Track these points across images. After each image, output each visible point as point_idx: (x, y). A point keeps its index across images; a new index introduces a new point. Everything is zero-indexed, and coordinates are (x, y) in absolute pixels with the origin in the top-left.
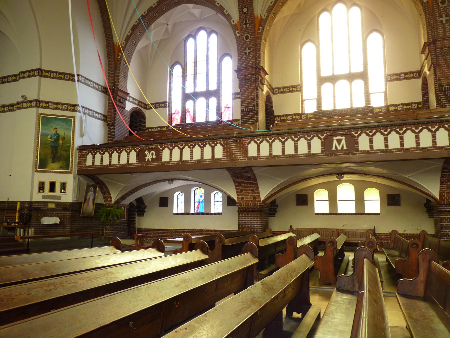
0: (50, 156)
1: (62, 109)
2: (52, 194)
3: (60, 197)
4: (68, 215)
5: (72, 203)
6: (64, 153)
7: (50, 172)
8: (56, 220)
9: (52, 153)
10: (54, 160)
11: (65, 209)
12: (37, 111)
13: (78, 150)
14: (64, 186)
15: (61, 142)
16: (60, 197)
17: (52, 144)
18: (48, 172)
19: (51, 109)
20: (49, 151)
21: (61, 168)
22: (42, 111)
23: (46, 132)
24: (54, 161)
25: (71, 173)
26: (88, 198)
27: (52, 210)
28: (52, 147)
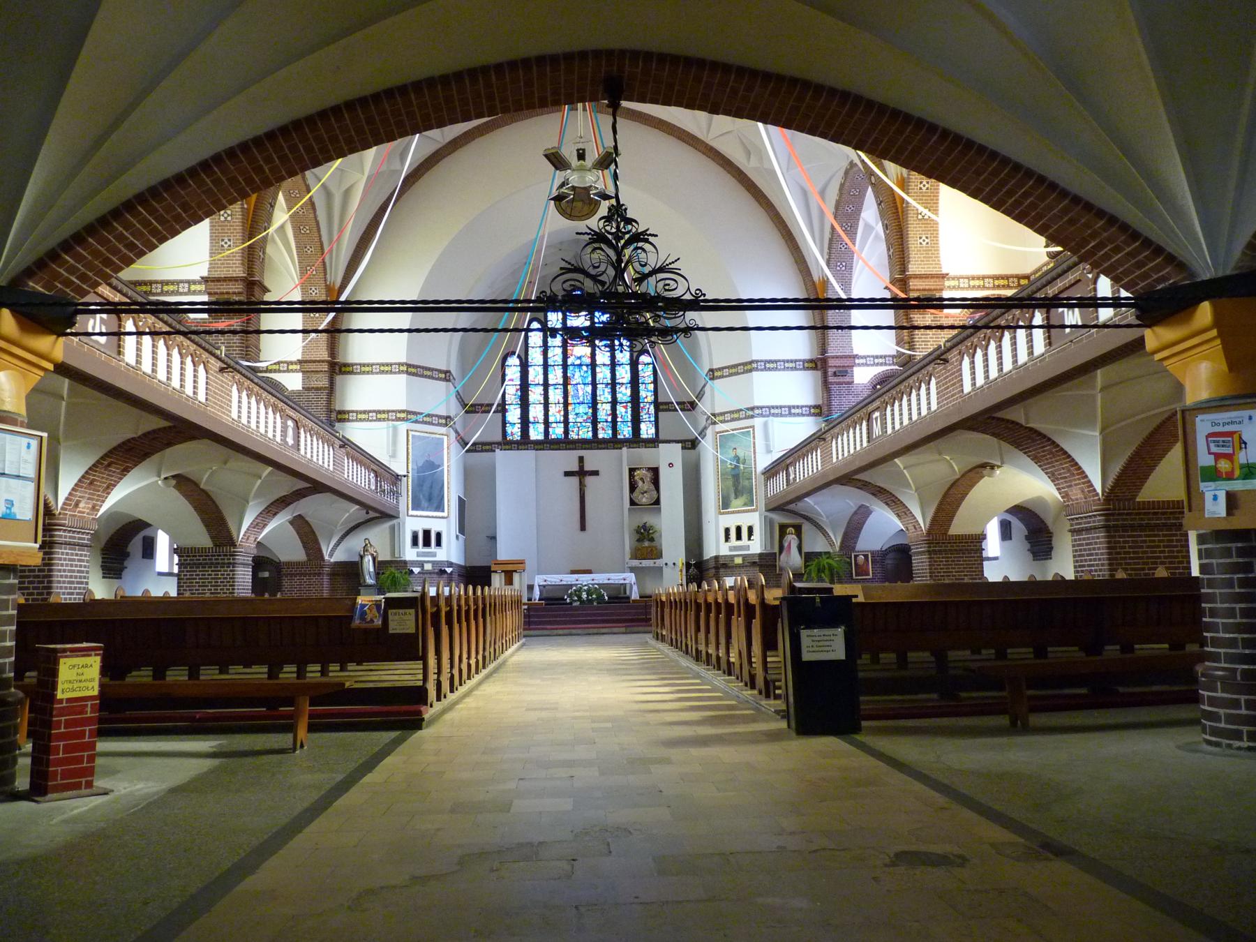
0: (732, 490)
1: (739, 419)
2: (739, 543)
3: (748, 548)
5: (760, 555)
6: (746, 483)
7: (739, 512)
11: (754, 563)
13: (763, 474)
14: (750, 530)
16: (748, 548)
18: (733, 512)
20: (730, 483)
21: (745, 505)
22: (720, 427)
24: (736, 497)
26: (786, 545)
27: (739, 566)
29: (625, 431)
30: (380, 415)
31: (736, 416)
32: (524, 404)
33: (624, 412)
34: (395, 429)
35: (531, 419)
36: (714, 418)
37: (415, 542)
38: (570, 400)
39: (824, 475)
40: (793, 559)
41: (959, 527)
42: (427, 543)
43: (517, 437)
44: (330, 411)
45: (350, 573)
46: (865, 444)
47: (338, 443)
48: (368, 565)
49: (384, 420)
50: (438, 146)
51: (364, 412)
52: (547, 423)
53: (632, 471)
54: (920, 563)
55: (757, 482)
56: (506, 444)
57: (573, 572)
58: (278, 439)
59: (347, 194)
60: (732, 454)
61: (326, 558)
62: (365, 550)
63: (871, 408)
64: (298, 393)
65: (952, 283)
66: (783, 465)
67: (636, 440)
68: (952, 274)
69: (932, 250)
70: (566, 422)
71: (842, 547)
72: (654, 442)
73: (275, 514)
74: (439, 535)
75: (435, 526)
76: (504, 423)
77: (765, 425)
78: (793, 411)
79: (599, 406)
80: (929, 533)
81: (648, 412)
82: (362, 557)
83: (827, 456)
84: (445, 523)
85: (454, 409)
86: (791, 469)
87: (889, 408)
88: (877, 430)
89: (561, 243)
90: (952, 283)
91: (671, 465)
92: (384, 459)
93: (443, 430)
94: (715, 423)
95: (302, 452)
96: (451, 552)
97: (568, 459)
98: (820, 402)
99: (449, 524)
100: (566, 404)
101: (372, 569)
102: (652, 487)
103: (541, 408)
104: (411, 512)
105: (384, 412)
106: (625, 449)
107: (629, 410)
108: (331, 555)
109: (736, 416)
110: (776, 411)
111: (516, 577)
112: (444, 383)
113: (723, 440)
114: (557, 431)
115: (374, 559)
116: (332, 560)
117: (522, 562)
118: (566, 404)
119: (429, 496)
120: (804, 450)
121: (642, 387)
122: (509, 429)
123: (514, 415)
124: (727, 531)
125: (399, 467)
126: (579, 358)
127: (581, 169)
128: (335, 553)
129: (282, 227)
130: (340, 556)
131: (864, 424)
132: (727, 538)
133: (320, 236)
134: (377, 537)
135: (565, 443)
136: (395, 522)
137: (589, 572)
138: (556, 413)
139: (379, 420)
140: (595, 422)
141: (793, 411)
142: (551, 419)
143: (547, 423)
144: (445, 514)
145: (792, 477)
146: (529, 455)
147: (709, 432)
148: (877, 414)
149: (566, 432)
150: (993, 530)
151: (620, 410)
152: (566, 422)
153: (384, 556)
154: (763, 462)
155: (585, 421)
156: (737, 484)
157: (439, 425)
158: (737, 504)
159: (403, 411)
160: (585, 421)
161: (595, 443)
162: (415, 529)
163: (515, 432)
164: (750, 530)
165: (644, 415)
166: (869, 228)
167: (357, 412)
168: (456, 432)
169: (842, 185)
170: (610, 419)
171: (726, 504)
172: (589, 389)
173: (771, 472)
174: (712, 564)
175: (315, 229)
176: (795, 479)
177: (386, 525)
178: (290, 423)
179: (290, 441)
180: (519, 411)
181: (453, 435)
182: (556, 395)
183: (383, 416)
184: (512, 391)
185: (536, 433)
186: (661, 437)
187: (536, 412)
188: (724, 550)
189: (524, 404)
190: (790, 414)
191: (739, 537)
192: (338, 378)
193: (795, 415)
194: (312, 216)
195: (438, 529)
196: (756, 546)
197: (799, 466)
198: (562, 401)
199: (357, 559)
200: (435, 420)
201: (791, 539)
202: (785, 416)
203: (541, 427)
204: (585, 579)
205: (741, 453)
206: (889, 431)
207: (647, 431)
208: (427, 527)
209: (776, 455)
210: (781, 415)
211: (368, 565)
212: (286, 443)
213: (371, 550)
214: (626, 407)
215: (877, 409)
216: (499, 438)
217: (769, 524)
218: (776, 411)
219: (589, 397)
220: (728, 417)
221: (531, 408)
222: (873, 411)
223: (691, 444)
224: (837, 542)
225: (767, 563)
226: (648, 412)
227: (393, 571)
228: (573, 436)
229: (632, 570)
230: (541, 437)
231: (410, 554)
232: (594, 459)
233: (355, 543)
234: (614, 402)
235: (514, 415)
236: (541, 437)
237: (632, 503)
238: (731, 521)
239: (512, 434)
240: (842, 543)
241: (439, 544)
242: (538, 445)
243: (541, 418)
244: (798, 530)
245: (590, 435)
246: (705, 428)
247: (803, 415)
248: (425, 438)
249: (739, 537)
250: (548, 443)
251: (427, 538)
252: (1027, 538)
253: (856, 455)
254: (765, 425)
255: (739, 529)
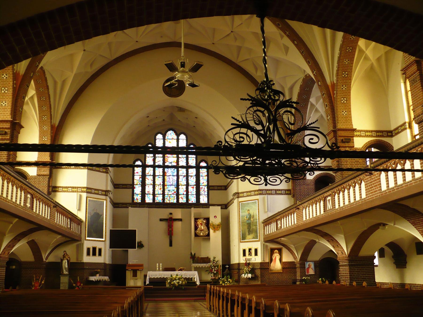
1: (251, 196)
4: (258, 272)
5: (261, 264)
6: (254, 227)
8: (250, 276)
9: (248, 228)
10: (250, 232)
12: (238, 200)
14: (256, 250)
15: (252, 219)
17: (248, 222)
18: (247, 242)
19: (245, 197)
20: (246, 227)
21: (253, 238)
22: (241, 199)
23: (244, 214)
24: (249, 234)
25: (257, 241)
26: (274, 258)
28: (248, 224)
29: (193, 199)
30: (74, 189)
31: (249, 194)
32: (143, 185)
33: (192, 191)
34: (81, 196)
35: (147, 192)
36: (237, 195)
37: (88, 254)
38: (166, 183)
39: (298, 226)
40: (277, 265)
41: (364, 252)
42: (94, 254)
43: (139, 201)
44: (49, 186)
45: (56, 267)
46: (322, 212)
47: (52, 205)
48: (65, 264)
49: (75, 192)
50: (109, 61)
51: (66, 187)
52: (154, 195)
53: (196, 219)
54: (344, 271)
55: (260, 227)
56: (134, 205)
57: (166, 269)
58: (22, 204)
59: (64, 82)
60: (246, 213)
61: (44, 260)
62: (64, 256)
63: (326, 195)
64: (35, 177)
65: (358, 133)
66: (274, 219)
67: (198, 204)
68: (358, 128)
69: (349, 118)
70: (164, 194)
71: (301, 259)
72: (207, 206)
73: (19, 240)
74: (100, 250)
75: (98, 245)
76: (133, 194)
77: (264, 199)
78: (277, 192)
79: (180, 187)
80: (349, 255)
81: (204, 190)
82: (62, 260)
83: (300, 217)
84: (103, 243)
85: (110, 187)
86: (279, 222)
87: (337, 196)
88: (329, 206)
89: (165, 108)
90: (358, 133)
91: (215, 217)
92: (74, 211)
93: (104, 197)
94: (238, 197)
95: (34, 211)
96: (105, 258)
97: (164, 213)
98: (290, 188)
99: (105, 244)
100: (164, 185)
101: (67, 267)
102: (206, 227)
103: (151, 187)
104: (87, 238)
105: (75, 188)
106: (192, 209)
107: (195, 189)
108: (47, 258)
109: (249, 194)
110: (269, 192)
111: (138, 273)
112: (105, 174)
113: (241, 205)
114: (159, 199)
115: (68, 261)
116: (47, 261)
117: (142, 266)
118: (164, 185)
119: (96, 230)
120: (287, 213)
121: (201, 178)
122: (135, 197)
123: (138, 190)
124: (244, 251)
125: (82, 215)
126: (171, 163)
127: (183, 72)
128: (49, 257)
129: (32, 97)
130: (51, 259)
131: (322, 202)
132: (244, 255)
133: (50, 102)
134: (70, 250)
135: (163, 205)
136: (79, 243)
137: (173, 270)
138: (159, 190)
139: (73, 192)
140: (178, 194)
141: (277, 192)
142: (156, 193)
143: (154, 195)
144: (104, 239)
145: (279, 226)
146: (145, 210)
147: (236, 201)
148: (329, 198)
149: (164, 199)
150: (376, 254)
151: (190, 189)
152: (164, 194)
153: (73, 260)
154: (264, 217)
155: (173, 194)
156: (249, 229)
157: (102, 195)
158: (249, 237)
159: (85, 188)
160: (173, 194)
161: (178, 205)
162: (89, 247)
163: (138, 198)
164: (256, 250)
165: (202, 192)
166: (312, 105)
167: (62, 187)
168: (110, 198)
169: (301, 85)
170: (185, 193)
171: (243, 238)
172: (175, 178)
173: (267, 222)
174: (236, 267)
175: (48, 98)
176: (281, 227)
177: (75, 244)
178: (29, 196)
179: (28, 205)
180: (140, 188)
181: (109, 200)
182: (159, 181)
183: (75, 190)
184: (137, 178)
185: (149, 199)
186: (210, 203)
187: (149, 189)
188: (242, 260)
189: (143, 185)
190: (276, 194)
191: (250, 254)
192: (54, 170)
193: (278, 194)
194: (46, 92)
195: (100, 247)
196: (257, 259)
197: (284, 221)
198: (162, 184)
199: (59, 261)
200: (100, 192)
201: (276, 256)
202: (274, 194)
203: (151, 197)
204: (174, 274)
205: (251, 212)
206: (337, 207)
207: (204, 199)
208: (94, 246)
209: (270, 214)
210: (272, 194)
211: (65, 264)
212: (27, 206)
213: (67, 257)
214: (193, 188)
215: (329, 195)
216: (130, 201)
217: (265, 247)
218: (269, 192)
219: (175, 182)
220: (245, 194)
221: (147, 187)
222: (327, 196)
223: (225, 206)
224: (299, 256)
225: (265, 267)
226: (204, 190)
227: (77, 267)
228: (167, 201)
229: (196, 269)
230: (151, 201)
231: (87, 259)
232: (178, 213)
233: (59, 253)
234: (187, 185)
235: (138, 190)
236: (151, 201)
237: (196, 235)
238: (246, 246)
239: (137, 199)
240: (301, 258)
241: (100, 254)
242: (150, 205)
243: (151, 192)
244: (280, 251)
245: (175, 201)
246: (233, 199)
247: (282, 194)
248: (94, 201)
249: (250, 254)
250: (154, 205)
251: (94, 251)
252: (393, 257)
253: (317, 218)
254: (264, 199)
255: (250, 250)
